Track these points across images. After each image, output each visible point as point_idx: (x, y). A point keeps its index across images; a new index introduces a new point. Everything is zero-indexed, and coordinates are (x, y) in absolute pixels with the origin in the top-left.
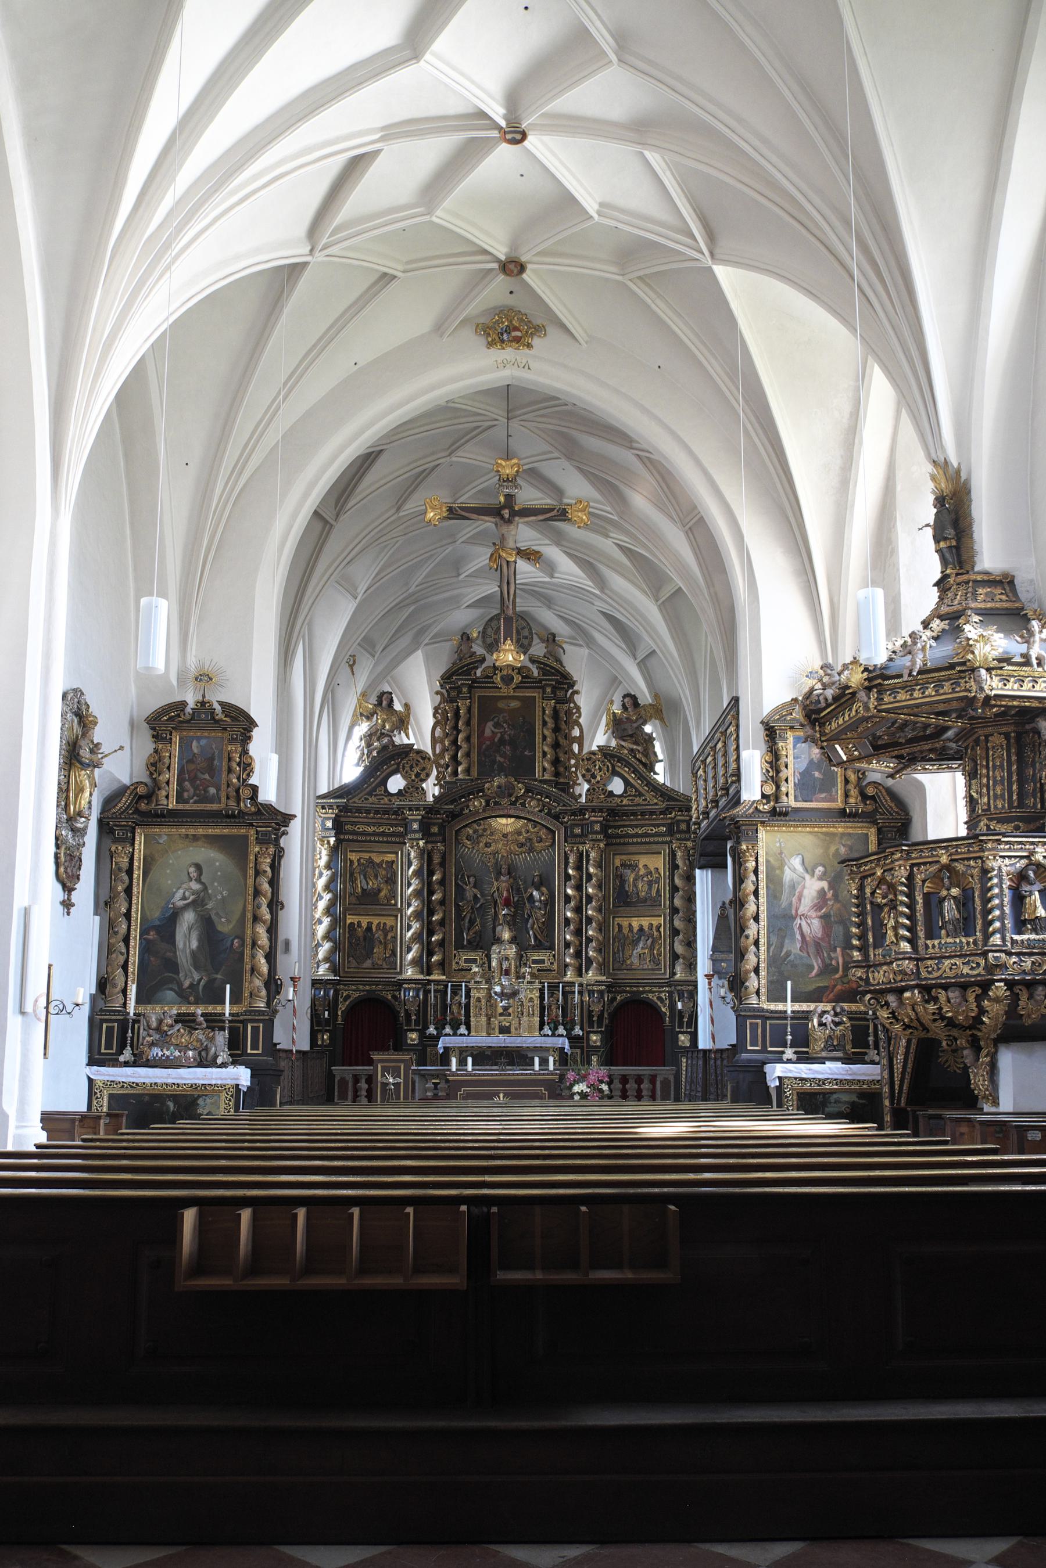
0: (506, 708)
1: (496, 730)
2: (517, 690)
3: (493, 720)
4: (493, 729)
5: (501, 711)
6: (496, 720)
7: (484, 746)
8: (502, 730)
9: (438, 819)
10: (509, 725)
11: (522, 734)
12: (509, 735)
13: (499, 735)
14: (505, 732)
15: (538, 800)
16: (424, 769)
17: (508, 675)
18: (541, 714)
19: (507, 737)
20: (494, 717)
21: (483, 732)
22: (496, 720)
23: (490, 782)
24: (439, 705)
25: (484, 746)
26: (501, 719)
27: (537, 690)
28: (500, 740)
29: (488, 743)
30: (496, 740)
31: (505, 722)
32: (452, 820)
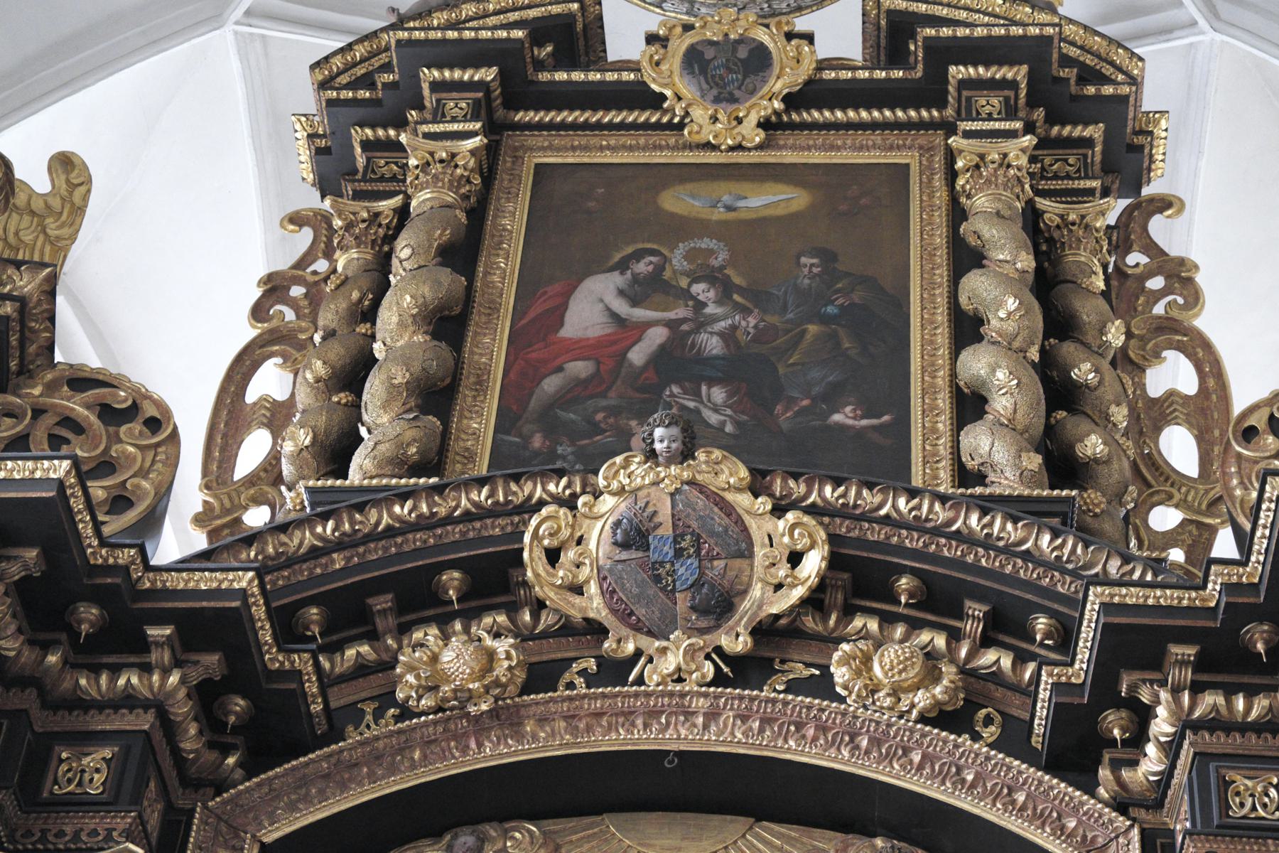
0: (719, 214)
1: (640, 314)
2: (783, 137)
3: (622, 266)
4: (621, 307)
5: (682, 228)
6: (643, 267)
7: (551, 384)
8: (679, 313)
9: (129, 701)
10: (726, 290)
11: (813, 329)
12: (728, 336)
13: (657, 336)
14: (701, 323)
15: (930, 655)
16: (106, 467)
17: (728, 46)
18: (940, 218)
19: (712, 344)
20: (638, 255)
21: (557, 315)
22: (643, 267)
23: (570, 503)
24: (302, 263)
25: (551, 384)
26: (678, 260)
27: (923, 138)
28: (662, 357)
29: (580, 368)
30: (637, 356)
31: (713, 277)
32: (251, 767)
